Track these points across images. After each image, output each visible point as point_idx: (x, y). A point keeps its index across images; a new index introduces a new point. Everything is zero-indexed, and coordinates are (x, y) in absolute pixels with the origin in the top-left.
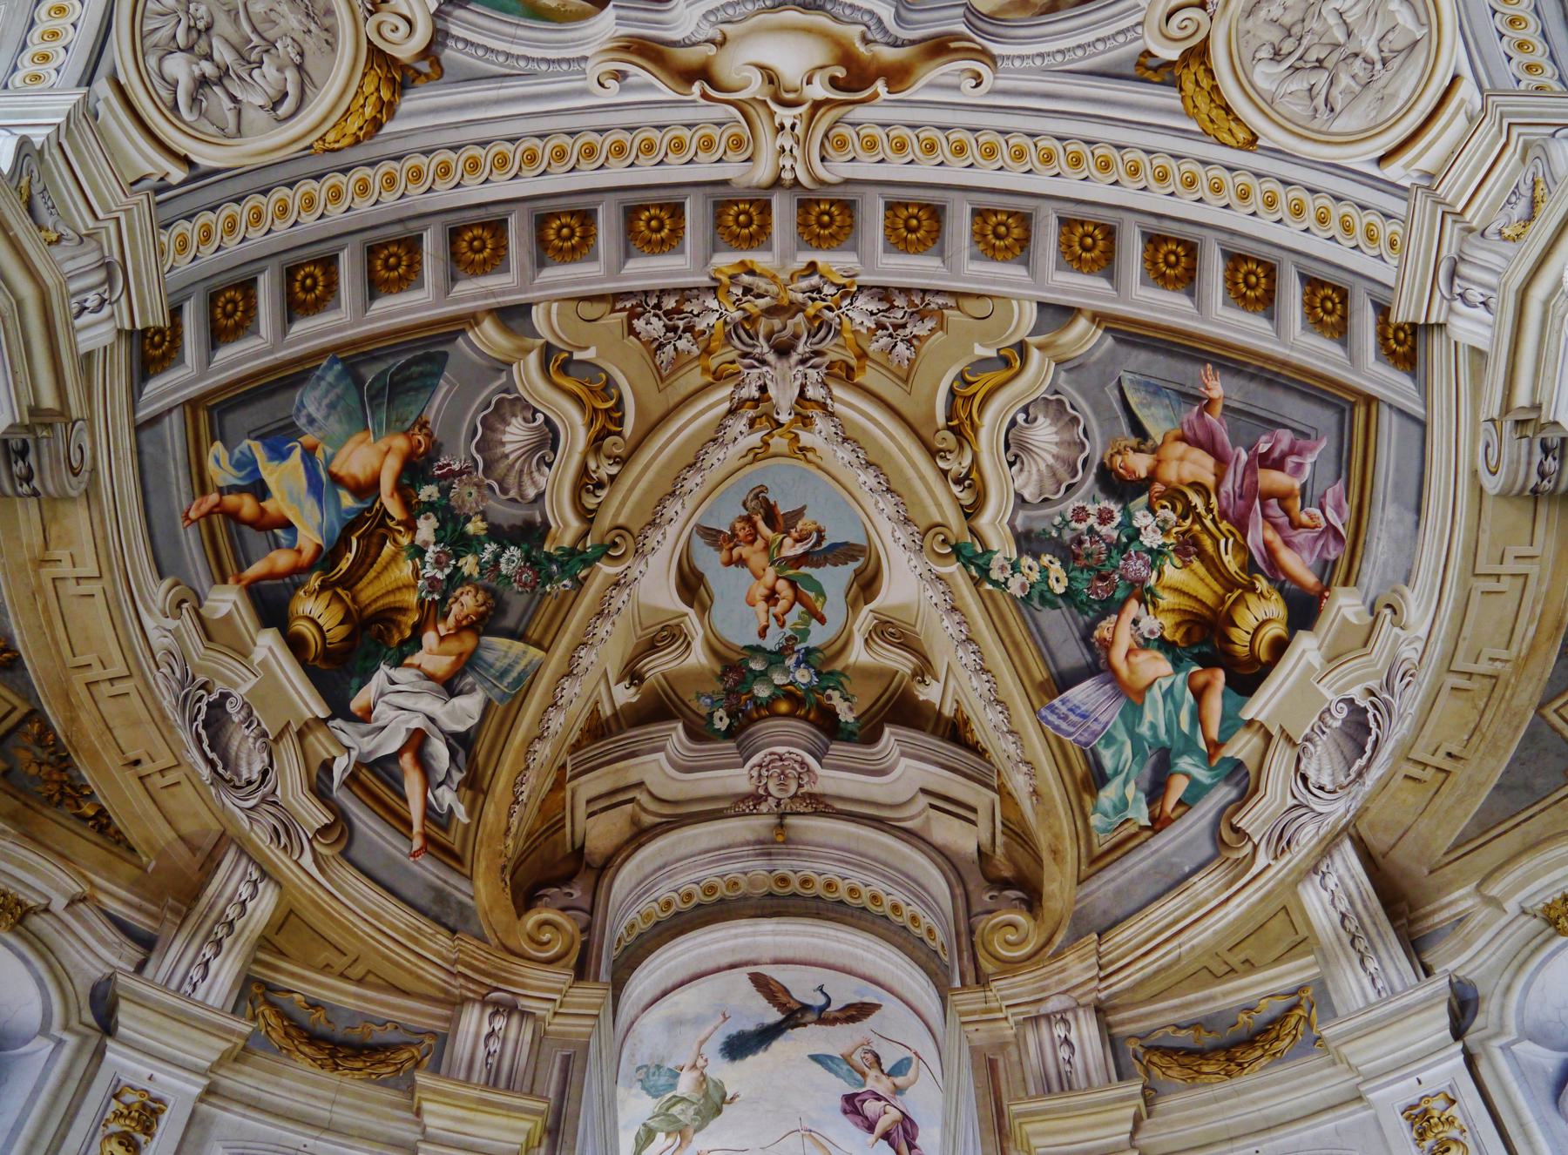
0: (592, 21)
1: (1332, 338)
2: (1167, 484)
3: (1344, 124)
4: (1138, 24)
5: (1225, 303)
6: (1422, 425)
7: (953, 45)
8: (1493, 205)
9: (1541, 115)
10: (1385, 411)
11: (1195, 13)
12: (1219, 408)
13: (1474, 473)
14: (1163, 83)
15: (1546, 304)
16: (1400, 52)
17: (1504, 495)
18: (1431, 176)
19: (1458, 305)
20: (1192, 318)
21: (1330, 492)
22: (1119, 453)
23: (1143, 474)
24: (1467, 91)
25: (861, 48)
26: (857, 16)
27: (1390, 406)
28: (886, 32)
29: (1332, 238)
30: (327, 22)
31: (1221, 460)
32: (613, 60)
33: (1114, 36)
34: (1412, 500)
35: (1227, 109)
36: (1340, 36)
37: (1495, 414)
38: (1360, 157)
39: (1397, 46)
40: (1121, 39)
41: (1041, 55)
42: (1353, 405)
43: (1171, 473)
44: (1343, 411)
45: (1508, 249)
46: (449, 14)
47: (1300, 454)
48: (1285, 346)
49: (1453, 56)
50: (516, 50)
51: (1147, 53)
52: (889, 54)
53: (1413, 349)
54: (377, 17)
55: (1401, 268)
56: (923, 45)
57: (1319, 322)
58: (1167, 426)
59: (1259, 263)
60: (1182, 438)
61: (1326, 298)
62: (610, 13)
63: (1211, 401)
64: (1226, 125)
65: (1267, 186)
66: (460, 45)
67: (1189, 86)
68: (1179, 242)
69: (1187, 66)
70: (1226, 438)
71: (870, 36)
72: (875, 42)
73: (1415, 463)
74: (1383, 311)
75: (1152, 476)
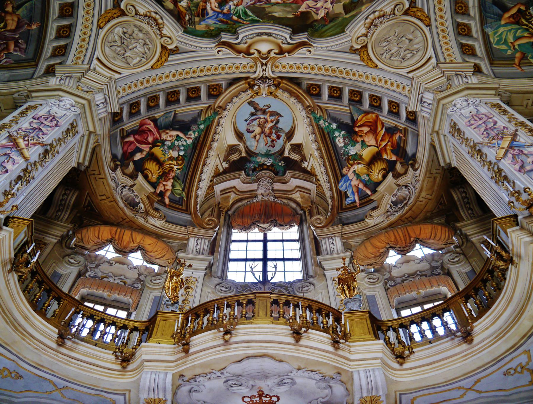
1: (52, 54)
2: (5, 17)
3: (107, 49)
5: (58, 26)
6: (31, 78)
8: (87, 84)
9: (111, 92)
10: (34, 69)
11: (134, 12)
12: (29, 28)
13: (19, 91)
14: (114, 5)
15: (58, 95)
16: (127, 61)
17: (14, 98)
18: (95, 69)
19: (59, 79)
20: (53, 18)
21: (10, 59)
22: (11, 2)
23: (7, 9)
24: (117, 76)
27: (35, 70)
29: (77, 50)
31: (14, 31)
34: (11, 79)
35: (109, 21)
36: (130, 47)
37: (29, 89)
38: (98, 53)
39: (128, 61)
42: (35, 61)
43: (9, 17)
44: (33, 59)
45: (75, 87)
47: (20, 51)
48: (49, 42)
49: (126, 72)
53: (50, 73)
55: (70, 65)
57: (56, 50)
58: (21, 15)
59: (69, 33)
60: (19, 19)
61: (62, 51)
63: (31, 26)
64: (104, 21)
65: (89, 32)
67: (114, 11)
68: (72, 12)
69: (119, 11)
70: (21, 31)
73: (20, 78)
74: (60, 63)
75: (7, 13)
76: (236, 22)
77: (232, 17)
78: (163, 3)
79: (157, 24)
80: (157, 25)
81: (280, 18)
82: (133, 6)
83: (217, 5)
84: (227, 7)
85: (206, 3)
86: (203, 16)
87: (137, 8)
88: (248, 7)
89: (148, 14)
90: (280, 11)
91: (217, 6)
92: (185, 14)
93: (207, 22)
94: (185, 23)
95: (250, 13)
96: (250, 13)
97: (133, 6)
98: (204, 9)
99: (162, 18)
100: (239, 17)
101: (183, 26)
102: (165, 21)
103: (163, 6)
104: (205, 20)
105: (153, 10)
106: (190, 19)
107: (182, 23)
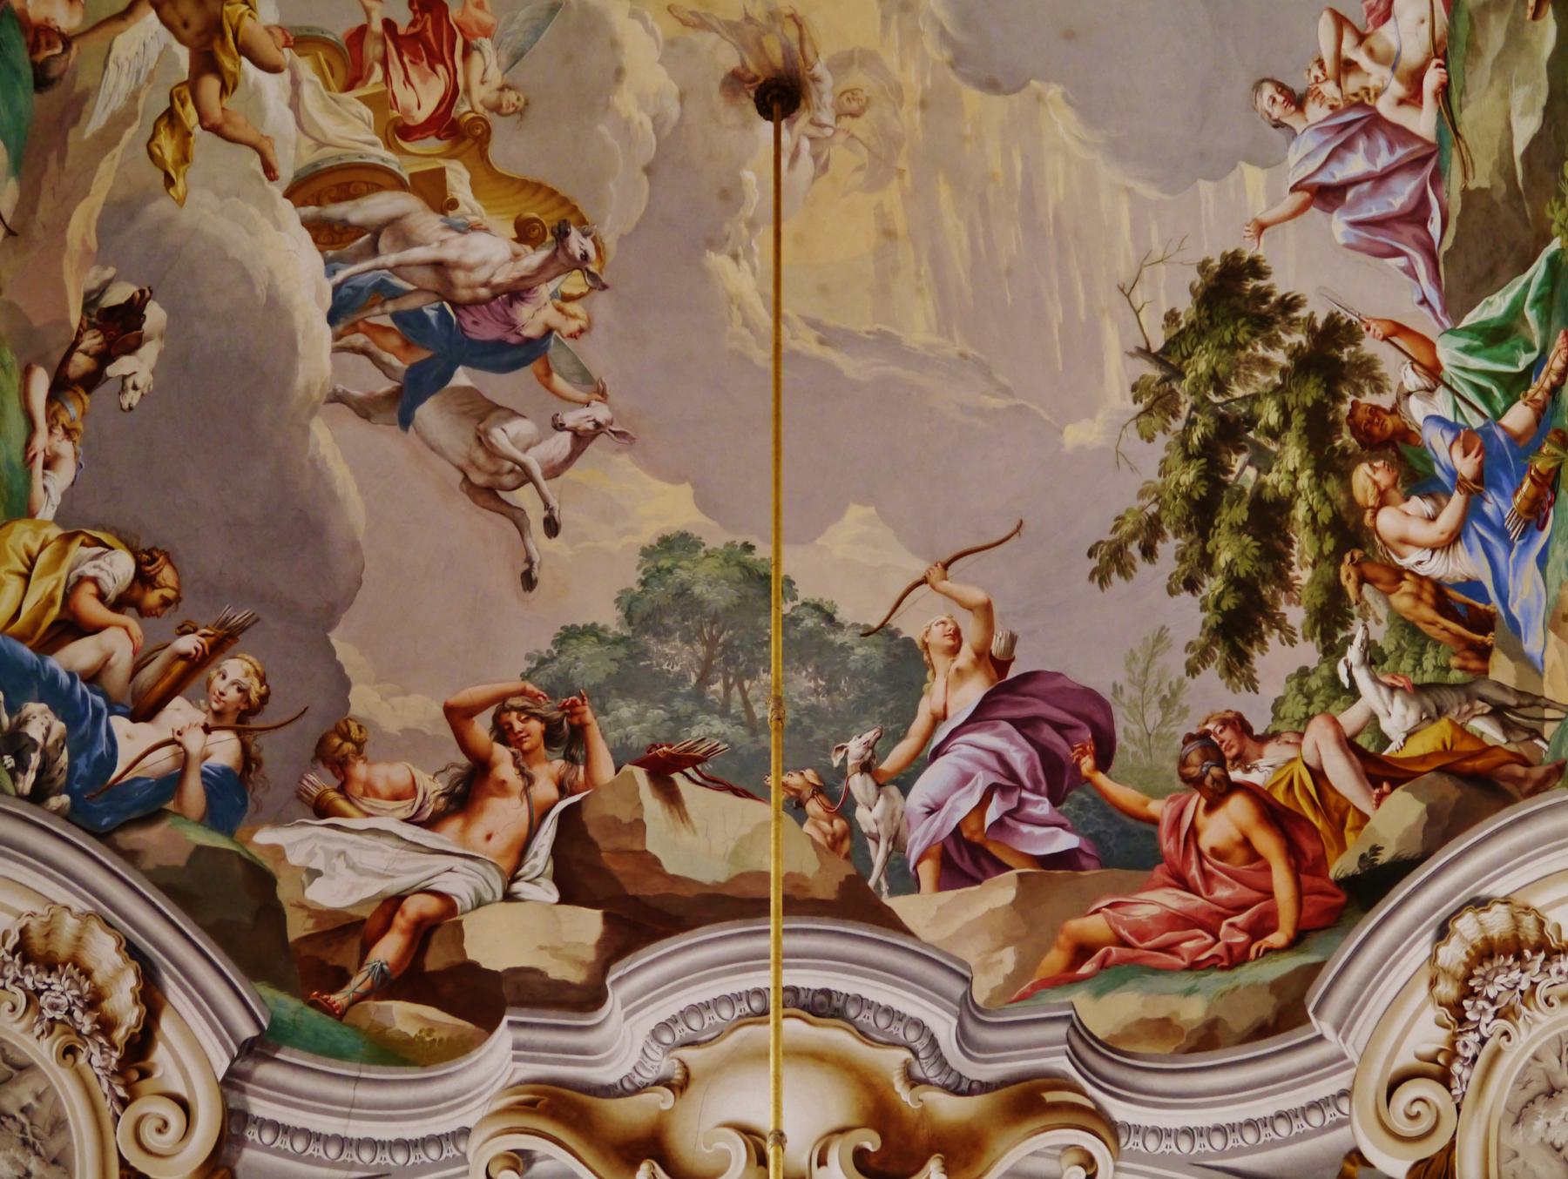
0: (476, 1055)
4: (1344, 1094)
7: (1051, 1097)
25: (904, 1095)
26: (898, 1030)
28: (942, 1062)
30: (54, 1146)
32: (510, 1131)
33: (1303, 1112)
40: (1315, 1119)
41: (1188, 1132)
46: (247, 1076)
50: (357, 1129)
51: (1356, 1156)
52: (949, 1109)
54: (135, 1110)
56: (1004, 1092)
62: (503, 1037)
66: (267, 1137)
71: (918, 1071)
72: (926, 1082)
76: (1544, 412)
77: (1514, 438)
78: (1384, 857)
79: (1513, 948)
80: (1519, 957)
81: (1548, 111)
82: (1393, 1087)
83: (1419, 505)
84: (1438, 442)
85: (1399, 574)
86: (1484, 622)
87: (1406, 1059)
88: (1456, 303)
89: (1447, 990)
90: (1505, 96)
91: (1427, 507)
92: (1462, 731)
93: (1527, 614)
94: (1526, 763)
95: (1494, 308)
96: (1494, 308)
97: (1393, 1087)
98: (1440, 595)
99: (1480, 904)
100: (1514, 385)
101: (1541, 786)
102: (1499, 888)
103: (1402, 868)
104: (1511, 619)
105: (1422, 949)
106: (1498, 712)
107: (1518, 781)
